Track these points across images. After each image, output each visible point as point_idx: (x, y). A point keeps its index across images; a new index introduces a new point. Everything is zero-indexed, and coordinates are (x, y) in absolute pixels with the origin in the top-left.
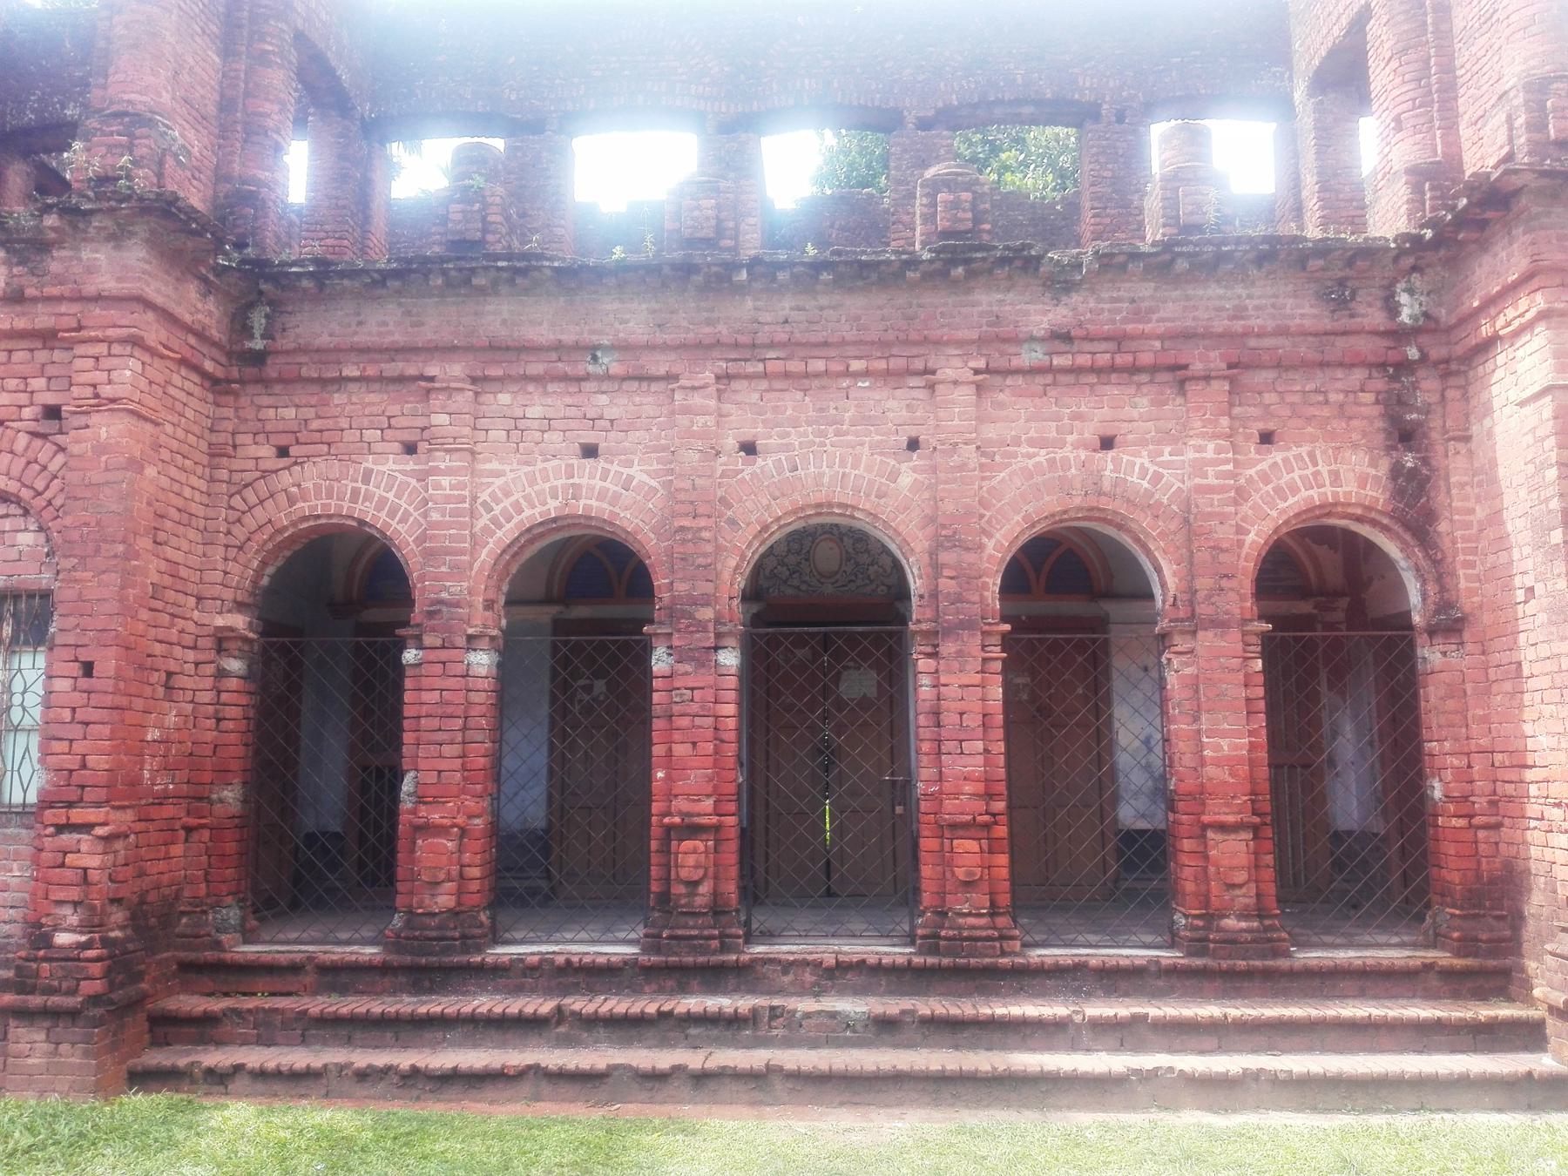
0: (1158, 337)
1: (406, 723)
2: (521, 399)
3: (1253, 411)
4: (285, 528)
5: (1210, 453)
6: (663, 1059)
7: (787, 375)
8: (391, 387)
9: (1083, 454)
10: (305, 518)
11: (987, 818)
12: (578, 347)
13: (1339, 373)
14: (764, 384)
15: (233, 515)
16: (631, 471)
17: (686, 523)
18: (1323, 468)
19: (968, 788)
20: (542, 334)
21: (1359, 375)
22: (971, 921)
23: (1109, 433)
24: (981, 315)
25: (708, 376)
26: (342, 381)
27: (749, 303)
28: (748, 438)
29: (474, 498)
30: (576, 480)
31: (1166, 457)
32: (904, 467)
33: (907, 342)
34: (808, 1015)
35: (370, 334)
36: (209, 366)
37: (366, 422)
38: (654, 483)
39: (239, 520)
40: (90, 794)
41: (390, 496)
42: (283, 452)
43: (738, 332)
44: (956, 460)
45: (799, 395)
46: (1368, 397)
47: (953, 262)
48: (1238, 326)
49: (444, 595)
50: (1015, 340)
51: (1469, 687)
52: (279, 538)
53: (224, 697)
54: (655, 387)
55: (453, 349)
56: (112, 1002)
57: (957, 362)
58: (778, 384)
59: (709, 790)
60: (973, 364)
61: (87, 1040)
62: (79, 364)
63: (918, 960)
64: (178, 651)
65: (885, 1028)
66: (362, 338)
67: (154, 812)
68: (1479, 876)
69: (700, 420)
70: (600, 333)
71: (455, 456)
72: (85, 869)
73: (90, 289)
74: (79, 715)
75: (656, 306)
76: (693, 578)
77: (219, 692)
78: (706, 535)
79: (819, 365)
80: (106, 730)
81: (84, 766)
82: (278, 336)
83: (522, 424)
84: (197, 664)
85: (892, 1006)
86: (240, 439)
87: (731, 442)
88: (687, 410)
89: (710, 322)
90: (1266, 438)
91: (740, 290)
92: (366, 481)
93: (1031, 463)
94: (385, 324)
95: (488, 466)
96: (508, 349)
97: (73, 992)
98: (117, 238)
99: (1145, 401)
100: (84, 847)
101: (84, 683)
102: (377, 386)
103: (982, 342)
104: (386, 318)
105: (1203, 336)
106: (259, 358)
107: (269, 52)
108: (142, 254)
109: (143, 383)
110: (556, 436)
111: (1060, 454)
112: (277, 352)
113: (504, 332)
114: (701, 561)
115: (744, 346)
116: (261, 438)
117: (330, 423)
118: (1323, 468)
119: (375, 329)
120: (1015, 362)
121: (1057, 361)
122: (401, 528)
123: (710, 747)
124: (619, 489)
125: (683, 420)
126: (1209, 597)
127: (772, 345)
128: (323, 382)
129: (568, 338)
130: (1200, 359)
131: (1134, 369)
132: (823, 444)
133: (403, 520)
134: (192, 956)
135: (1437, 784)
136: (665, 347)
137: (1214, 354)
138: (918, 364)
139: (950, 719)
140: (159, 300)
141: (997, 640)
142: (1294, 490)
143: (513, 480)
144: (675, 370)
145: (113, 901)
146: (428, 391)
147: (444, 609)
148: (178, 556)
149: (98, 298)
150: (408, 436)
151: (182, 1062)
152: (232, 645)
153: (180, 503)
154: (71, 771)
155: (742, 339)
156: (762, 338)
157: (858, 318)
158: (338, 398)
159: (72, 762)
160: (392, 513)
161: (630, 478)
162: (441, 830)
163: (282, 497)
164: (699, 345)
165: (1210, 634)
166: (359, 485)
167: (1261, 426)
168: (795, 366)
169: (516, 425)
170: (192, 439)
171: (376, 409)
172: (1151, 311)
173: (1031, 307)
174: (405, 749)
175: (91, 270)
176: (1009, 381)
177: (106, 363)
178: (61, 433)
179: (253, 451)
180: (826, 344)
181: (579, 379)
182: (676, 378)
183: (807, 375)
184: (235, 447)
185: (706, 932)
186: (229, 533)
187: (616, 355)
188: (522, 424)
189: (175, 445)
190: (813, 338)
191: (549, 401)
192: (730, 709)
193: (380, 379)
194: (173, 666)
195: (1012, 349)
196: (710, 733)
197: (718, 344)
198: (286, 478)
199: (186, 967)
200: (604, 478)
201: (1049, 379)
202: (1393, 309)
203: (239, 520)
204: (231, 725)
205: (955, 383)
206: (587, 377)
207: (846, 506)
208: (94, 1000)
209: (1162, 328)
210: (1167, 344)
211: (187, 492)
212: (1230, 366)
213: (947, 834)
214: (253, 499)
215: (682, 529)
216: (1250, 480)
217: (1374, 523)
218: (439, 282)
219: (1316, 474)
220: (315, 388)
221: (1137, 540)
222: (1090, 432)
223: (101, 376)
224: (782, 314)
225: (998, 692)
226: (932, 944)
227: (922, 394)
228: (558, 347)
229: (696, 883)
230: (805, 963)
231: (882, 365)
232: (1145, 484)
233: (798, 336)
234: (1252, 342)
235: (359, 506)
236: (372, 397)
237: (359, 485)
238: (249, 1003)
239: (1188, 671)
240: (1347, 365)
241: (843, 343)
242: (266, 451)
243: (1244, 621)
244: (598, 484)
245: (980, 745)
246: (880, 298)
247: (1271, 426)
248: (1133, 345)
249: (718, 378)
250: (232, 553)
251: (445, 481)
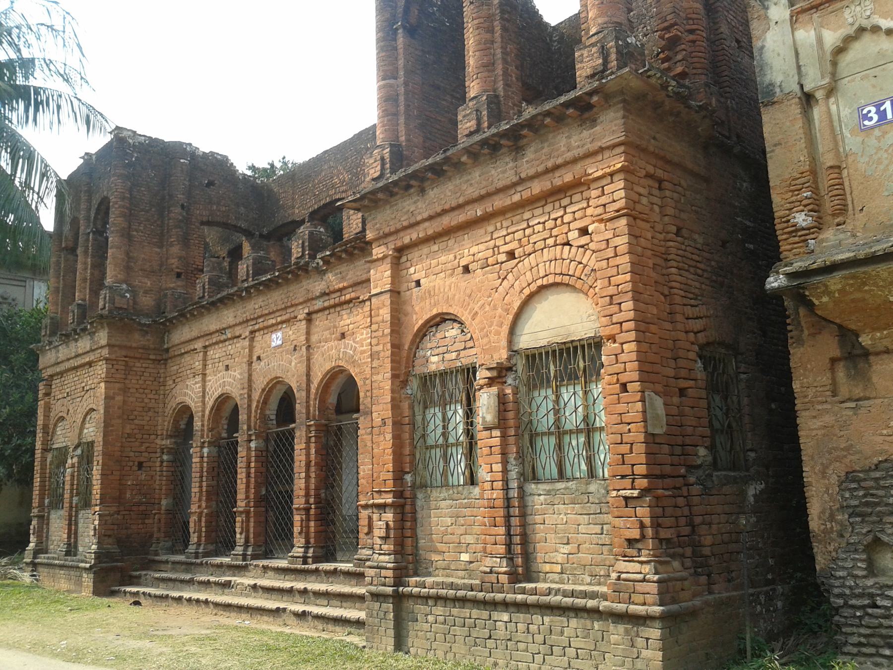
36: (152, 357)
64: (146, 454)
66: (182, 339)
67: (134, 508)
87: (255, 358)
96: (207, 335)
106: (167, 350)
109: (113, 371)
140: (118, 343)
145: (105, 536)
148: (141, 423)
153: (143, 404)
158: (183, 360)
164: (244, 322)
170: (150, 383)
189: (138, 386)
194: (142, 459)
197: (247, 321)
206: (225, 341)
211: (146, 401)
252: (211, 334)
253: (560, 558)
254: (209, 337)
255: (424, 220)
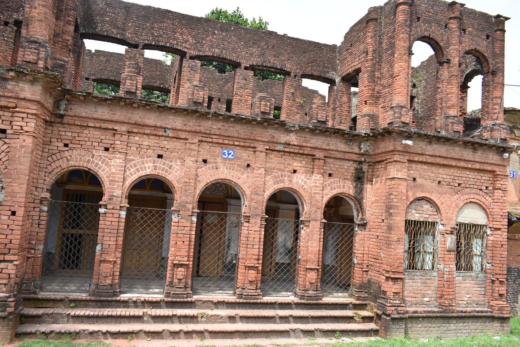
0: (310, 147)
1: (99, 230)
2: (142, 139)
3: (328, 168)
4: (65, 168)
5: (318, 178)
6: (176, 327)
7: (217, 143)
8: (102, 131)
9: (289, 174)
10: (72, 166)
11: (258, 265)
12: (161, 127)
13: (347, 162)
14: (211, 144)
15: (49, 163)
16: (172, 164)
17: (187, 181)
18: (341, 184)
19: (254, 257)
20: (151, 122)
21: (352, 163)
22: (251, 291)
23: (295, 169)
24: (269, 135)
25: (196, 141)
26: (88, 126)
27: (210, 122)
28: (205, 158)
29: (125, 166)
30: (156, 164)
31: (308, 177)
32: (246, 171)
33: (250, 139)
34: (212, 316)
35: (99, 114)
37: (94, 140)
38: (178, 168)
39: (50, 164)
40: (12, 251)
41: (100, 163)
42: (66, 145)
43: (206, 130)
44: (259, 172)
45: (220, 149)
46: (352, 168)
47: (265, 122)
48: (328, 148)
49: (115, 194)
50: (277, 143)
51: (365, 238)
52: (62, 171)
53: (41, 218)
54: (181, 141)
55: (123, 123)
56: (16, 314)
57: (262, 146)
58: (215, 145)
59: (187, 255)
60: (266, 147)
61: (8, 325)
62: (16, 119)
63: (238, 300)
65: (232, 319)
66: (95, 116)
68: (363, 283)
69: (193, 152)
70: (168, 124)
71: (122, 154)
72: (9, 274)
73: (22, 96)
74: (10, 227)
75: (184, 119)
76: (188, 196)
77: (40, 216)
78: (192, 184)
79: (226, 142)
80: (19, 232)
81: (11, 242)
82: (69, 111)
83: (141, 146)
84: (34, 208)
85: (232, 312)
86: (52, 140)
87: (200, 159)
88: (190, 149)
89: (199, 126)
90: (330, 175)
91: (209, 119)
92: (93, 157)
93: (277, 174)
94: (104, 112)
95: (130, 157)
96: (140, 125)
97: (4, 311)
98: (33, 82)
99: (304, 162)
100: (9, 268)
101: (12, 217)
102: (98, 130)
103: (268, 142)
104: (104, 111)
105: (319, 149)
106: (62, 116)
107: (70, 21)
108: (40, 88)
110: (152, 151)
111: (283, 173)
112: (68, 116)
113: (140, 120)
114: (190, 191)
115: (208, 134)
116: (59, 140)
117: (82, 139)
118: (341, 184)
119: (100, 113)
120: (276, 148)
121: (286, 150)
122: (103, 173)
123: (188, 243)
124: (168, 169)
125: (189, 152)
126: (314, 213)
127: (215, 135)
128: (81, 126)
129: (158, 124)
130: (319, 154)
131: (303, 154)
132: (225, 163)
133: (103, 171)
134: (28, 296)
135: (355, 259)
136: (185, 131)
137: (321, 153)
138: (252, 145)
139: (251, 239)
141: (264, 219)
142: (335, 189)
143: (137, 162)
144: (187, 137)
146: (115, 134)
147: (114, 198)
149: (24, 99)
150: (107, 146)
151: (34, 330)
152: (45, 203)
154: (6, 244)
155: (207, 132)
156: (212, 132)
157: (238, 131)
158: (86, 132)
159: (7, 241)
160: (100, 168)
161: (171, 166)
162: (110, 262)
163: (65, 159)
164: (195, 132)
165: (313, 222)
166: (90, 158)
167: (329, 172)
168: (220, 141)
169: (139, 146)
171: (97, 137)
172: (309, 141)
173: (281, 135)
174: (98, 237)
175: (22, 90)
176: (274, 153)
177: (25, 120)
178: (6, 138)
179: (57, 144)
180: (229, 136)
181: (159, 136)
182: (187, 139)
183: (223, 144)
184: (51, 142)
185: (183, 293)
186: (46, 168)
187: (171, 131)
188: (141, 146)
190: (226, 135)
191: (150, 141)
192: (194, 233)
193: (100, 128)
195: (276, 145)
196: (188, 239)
197: (201, 132)
198: (67, 154)
199: (25, 299)
200: (164, 165)
201: (283, 153)
202: (360, 149)
203: (50, 164)
204: (43, 226)
205: (261, 152)
206: (162, 136)
207: (229, 180)
208: (10, 314)
209: (310, 145)
210: (311, 149)
212: (325, 157)
213: (247, 269)
214: (55, 159)
215: (186, 182)
216: (326, 185)
217: (350, 198)
218: (123, 104)
219: (340, 185)
220: (78, 128)
221: (299, 196)
222: (291, 169)
223: (23, 124)
224: (219, 127)
225: (263, 233)
226: (240, 296)
227: (252, 153)
228: (155, 127)
229: (181, 280)
230: (209, 301)
231: (243, 144)
232: (303, 183)
233: (222, 133)
234: (330, 152)
235: (89, 165)
236: (96, 133)
237: (90, 158)
238: (50, 311)
239: (308, 230)
240: (349, 160)
241: (234, 137)
242: (61, 145)
243: (321, 219)
244: (162, 166)
245: (258, 247)
246: (245, 127)
247: (331, 172)
248: (303, 148)
249: (199, 141)
250: (47, 174)
251: (118, 161)
252: (143, 126)
253: (466, 299)
254: (141, 127)
255: (429, 155)
